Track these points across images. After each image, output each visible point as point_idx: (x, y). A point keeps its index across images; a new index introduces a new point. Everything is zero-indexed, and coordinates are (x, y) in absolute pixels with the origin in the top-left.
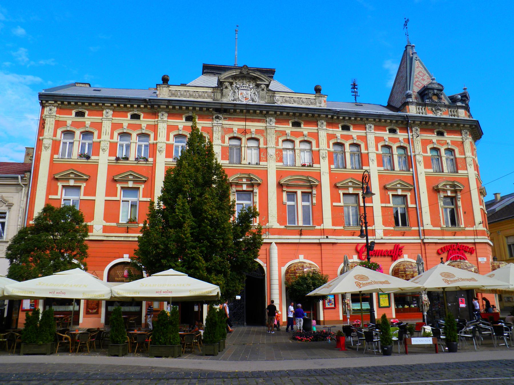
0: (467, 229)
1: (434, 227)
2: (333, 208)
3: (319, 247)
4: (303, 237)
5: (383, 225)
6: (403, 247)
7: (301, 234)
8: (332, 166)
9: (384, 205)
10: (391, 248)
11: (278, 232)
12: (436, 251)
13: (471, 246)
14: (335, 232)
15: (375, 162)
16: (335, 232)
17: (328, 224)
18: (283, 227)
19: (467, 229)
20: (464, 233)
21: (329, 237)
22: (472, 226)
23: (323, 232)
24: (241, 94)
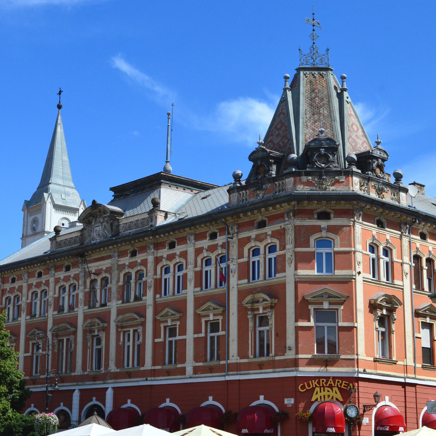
0: (277, 358)
1: (241, 358)
2: (155, 345)
5: (194, 360)
7: (130, 377)
8: (158, 296)
9: (196, 336)
11: (116, 376)
14: (153, 373)
15: (193, 284)
16: (153, 373)
18: (118, 370)
19: (277, 358)
20: (274, 365)
22: (283, 355)
24: (96, 231)
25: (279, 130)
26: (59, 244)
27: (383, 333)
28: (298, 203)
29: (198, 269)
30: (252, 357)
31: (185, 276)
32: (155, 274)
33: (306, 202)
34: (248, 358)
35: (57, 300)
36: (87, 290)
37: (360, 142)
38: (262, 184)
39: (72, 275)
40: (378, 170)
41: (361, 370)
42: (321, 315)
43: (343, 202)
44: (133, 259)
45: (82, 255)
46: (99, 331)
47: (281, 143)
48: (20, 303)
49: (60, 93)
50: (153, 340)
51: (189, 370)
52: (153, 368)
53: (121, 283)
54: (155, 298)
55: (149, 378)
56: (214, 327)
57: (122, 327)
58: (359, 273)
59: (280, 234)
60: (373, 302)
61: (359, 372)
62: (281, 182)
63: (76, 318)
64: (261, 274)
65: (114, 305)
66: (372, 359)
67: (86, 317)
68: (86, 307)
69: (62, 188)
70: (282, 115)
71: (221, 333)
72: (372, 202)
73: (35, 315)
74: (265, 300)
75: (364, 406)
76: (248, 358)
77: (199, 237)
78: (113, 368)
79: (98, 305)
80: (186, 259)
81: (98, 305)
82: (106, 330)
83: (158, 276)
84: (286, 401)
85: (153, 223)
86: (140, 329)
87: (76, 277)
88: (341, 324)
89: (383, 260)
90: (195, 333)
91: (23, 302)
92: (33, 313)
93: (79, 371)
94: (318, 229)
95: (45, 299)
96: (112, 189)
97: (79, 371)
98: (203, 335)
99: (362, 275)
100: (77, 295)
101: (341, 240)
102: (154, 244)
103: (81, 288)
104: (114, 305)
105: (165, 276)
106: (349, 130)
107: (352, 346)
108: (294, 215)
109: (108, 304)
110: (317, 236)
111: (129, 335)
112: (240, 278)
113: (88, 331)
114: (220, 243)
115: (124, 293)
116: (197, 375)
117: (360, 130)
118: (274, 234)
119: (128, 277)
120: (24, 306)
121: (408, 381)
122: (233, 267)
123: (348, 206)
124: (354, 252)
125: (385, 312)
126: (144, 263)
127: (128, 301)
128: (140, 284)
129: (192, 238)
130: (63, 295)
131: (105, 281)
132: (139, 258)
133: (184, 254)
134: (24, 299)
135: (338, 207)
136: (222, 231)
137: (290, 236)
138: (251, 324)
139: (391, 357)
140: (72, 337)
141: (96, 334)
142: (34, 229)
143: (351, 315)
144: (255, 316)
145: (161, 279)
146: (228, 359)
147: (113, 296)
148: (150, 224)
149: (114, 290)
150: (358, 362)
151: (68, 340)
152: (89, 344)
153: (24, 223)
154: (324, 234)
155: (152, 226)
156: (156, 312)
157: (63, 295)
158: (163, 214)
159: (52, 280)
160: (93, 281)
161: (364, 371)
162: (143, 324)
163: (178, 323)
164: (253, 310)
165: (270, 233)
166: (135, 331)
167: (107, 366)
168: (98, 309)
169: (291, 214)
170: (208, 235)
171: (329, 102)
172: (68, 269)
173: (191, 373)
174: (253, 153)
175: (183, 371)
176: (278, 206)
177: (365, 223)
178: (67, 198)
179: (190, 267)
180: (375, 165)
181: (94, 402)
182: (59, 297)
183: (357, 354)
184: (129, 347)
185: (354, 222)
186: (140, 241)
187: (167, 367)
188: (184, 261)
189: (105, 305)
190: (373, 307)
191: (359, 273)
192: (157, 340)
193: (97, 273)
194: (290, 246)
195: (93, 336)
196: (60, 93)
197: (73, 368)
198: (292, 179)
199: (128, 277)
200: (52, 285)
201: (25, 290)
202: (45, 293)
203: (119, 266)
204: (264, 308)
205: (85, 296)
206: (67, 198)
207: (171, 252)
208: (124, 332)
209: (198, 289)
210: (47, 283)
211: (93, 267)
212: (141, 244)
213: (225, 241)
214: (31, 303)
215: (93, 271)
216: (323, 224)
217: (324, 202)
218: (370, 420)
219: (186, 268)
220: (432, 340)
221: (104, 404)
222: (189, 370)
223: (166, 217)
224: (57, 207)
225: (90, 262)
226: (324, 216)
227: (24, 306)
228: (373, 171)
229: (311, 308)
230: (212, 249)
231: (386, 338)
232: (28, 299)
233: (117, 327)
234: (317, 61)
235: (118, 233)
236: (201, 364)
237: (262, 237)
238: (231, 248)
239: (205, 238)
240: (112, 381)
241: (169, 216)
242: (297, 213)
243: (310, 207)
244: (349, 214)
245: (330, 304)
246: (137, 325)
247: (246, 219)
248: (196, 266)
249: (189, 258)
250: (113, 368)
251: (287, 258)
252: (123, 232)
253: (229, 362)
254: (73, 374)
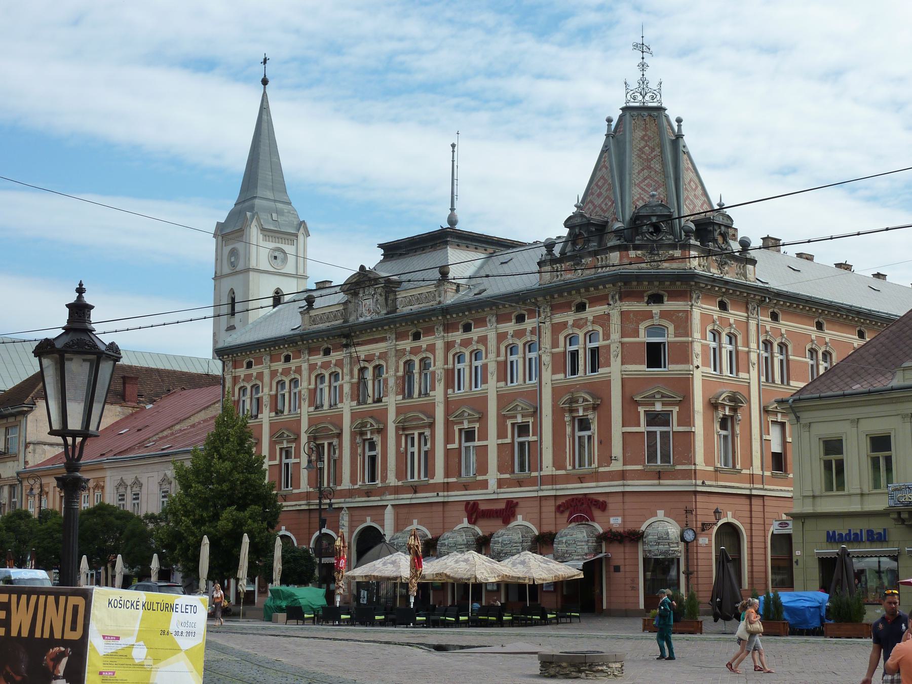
0: (601, 469)
1: (557, 469)
2: (447, 452)
3: (441, 508)
4: (418, 495)
5: (498, 471)
6: (517, 503)
7: (415, 492)
8: (450, 391)
9: (500, 441)
10: (502, 506)
11: (396, 490)
12: (553, 509)
13: (601, 499)
14: (447, 487)
15: (495, 377)
16: (447, 487)
17: (439, 477)
18: (400, 483)
19: (601, 469)
20: (596, 476)
21: (440, 494)
22: (608, 466)
23: (434, 488)
25: (600, 188)
26: (314, 321)
27: (725, 437)
28: (625, 284)
29: (502, 358)
30: (571, 468)
31: (485, 367)
32: (446, 362)
33: (635, 283)
34: (566, 469)
35: (313, 393)
36: (355, 380)
37: (699, 203)
38: (581, 258)
39: (334, 362)
40: (720, 240)
41: (699, 482)
42: (654, 419)
43: (678, 283)
44: (416, 344)
45: (347, 336)
46: (372, 433)
47: (603, 206)
48: (260, 395)
49: (265, 61)
50: (445, 446)
51: (492, 484)
52: (446, 480)
53: (401, 373)
54: (446, 393)
55: (440, 494)
56: (523, 429)
57: (404, 429)
58: (698, 367)
59: (603, 320)
60: (713, 402)
61: (696, 485)
62: (603, 256)
63: (341, 417)
64: (581, 368)
65: (392, 401)
66: (711, 469)
67: (354, 416)
68: (355, 403)
69: (272, 204)
70: (604, 169)
71: (531, 438)
72: (714, 280)
73: (282, 412)
74: (585, 400)
75: (703, 524)
76: (566, 469)
77: (501, 319)
78: (392, 480)
79: (370, 400)
80: (486, 346)
81: (370, 400)
82: (382, 431)
83: (450, 366)
84: (612, 520)
85: (442, 299)
86: (427, 432)
87: (339, 364)
88: (676, 428)
89: (727, 347)
90: (499, 437)
91: (265, 393)
92: (280, 407)
93: (346, 484)
95: (296, 390)
96: (380, 246)
97: (346, 484)
98: (509, 440)
99: (701, 369)
100: (341, 386)
101: (676, 328)
102: (444, 325)
103: (347, 378)
104: (392, 401)
105: (458, 366)
106: (686, 189)
107: (687, 453)
108: (621, 299)
109: (384, 399)
110: (648, 323)
111: (413, 439)
112: (554, 373)
113: (359, 432)
114: (529, 328)
115: (406, 385)
116: (502, 490)
117: (700, 187)
118: (597, 320)
119: (409, 364)
120: (266, 400)
121: (754, 492)
122: (546, 359)
124: (692, 342)
125: (728, 411)
126: (431, 348)
127: (410, 395)
128: (426, 374)
129: (494, 319)
130: (321, 386)
131: (378, 368)
132: (424, 342)
133: (483, 340)
134: (266, 390)
135: (672, 288)
136: (532, 314)
137: (615, 320)
138: (569, 430)
139: (734, 466)
140: (335, 442)
141: (369, 437)
142: (233, 265)
143: (687, 418)
144: (574, 418)
145: (454, 369)
146: (541, 469)
147: (389, 389)
148: (438, 299)
149: (391, 382)
150: (695, 473)
151: (330, 444)
152: (360, 450)
153: (217, 255)
154: (656, 321)
155: (440, 302)
156: (447, 413)
157: (321, 386)
158: (454, 287)
159: (305, 366)
160: (362, 370)
161: (703, 483)
162: (432, 425)
163: (477, 425)
164: (571, 411)
165: (591, 318)
166: (420, 434)
167: (384, 478)
168: (370, 406)
169: (617, 297)
170: (513, 317)
171: (662, 152)
172: (327, 352)
173: (496, 486)
174: (570, 218)
175: (484, 485)
176: (601, 287)
177: (704, 306)
178: (281, 220)
179: (492, 356)
180: (716, 233)
181: (369, 522)
182: (315, 389)
183: (695, 464)
184: (413, 453)
185: (692, 305)
186: (425, 321)
187: (464, 478)
188: (483, 348)
189: (379, 400)
190: (713, 405)
191: (698, 367)
192: (449, 446)
193: (368, 360)
194: (615, 336)
195: (364, 440)
196: (265, 61)
197: (337, 480)
198: (617, 254)
199: (409, 364)
200: (305, 373)
201: (266, 379)
202: (295, 382)
203: (397, 351)
204: (585, 410)
205: (352, 388)
206: (281, 220)
207: (467, 336)
208: (407, 436)
209: (502, 384)
210: (298, 370)
211: (363, 351)
212: (426, 325)
213: (535, 325)
214: (276, 395)
215: (363, 357)
216: (655, 309)
217: (656, 283)
218: (710, 540)
219: (486, 358)
220: (784, 443)
221: (383, 526)
222: (492, 484)
223: (457, 291)
225: (358, 344)
226: (657, 299)
227: (266, 400)
228: (715, 241)
229: (641, 410)
230: (519, 334)
231: (728, 442)
232: (271, 390)
233: (397, 429)
234: (647, 98)
235: (395, 310)
236: (507, 476)
237: (582, 322)
238: (543, 335)
239: (510, 321)
240: (392, 497)
241: (461, 288)
242: (624, 296)
243: (640, 289)
245: (663, 404)
246: (424, 427)
247: (562, 300)
248: (498, 355)
249: (489, 344)
250: (392, 480)
251: (612, 350)
252: (404, 310)
253: (542, 473)
254: (339, 488)
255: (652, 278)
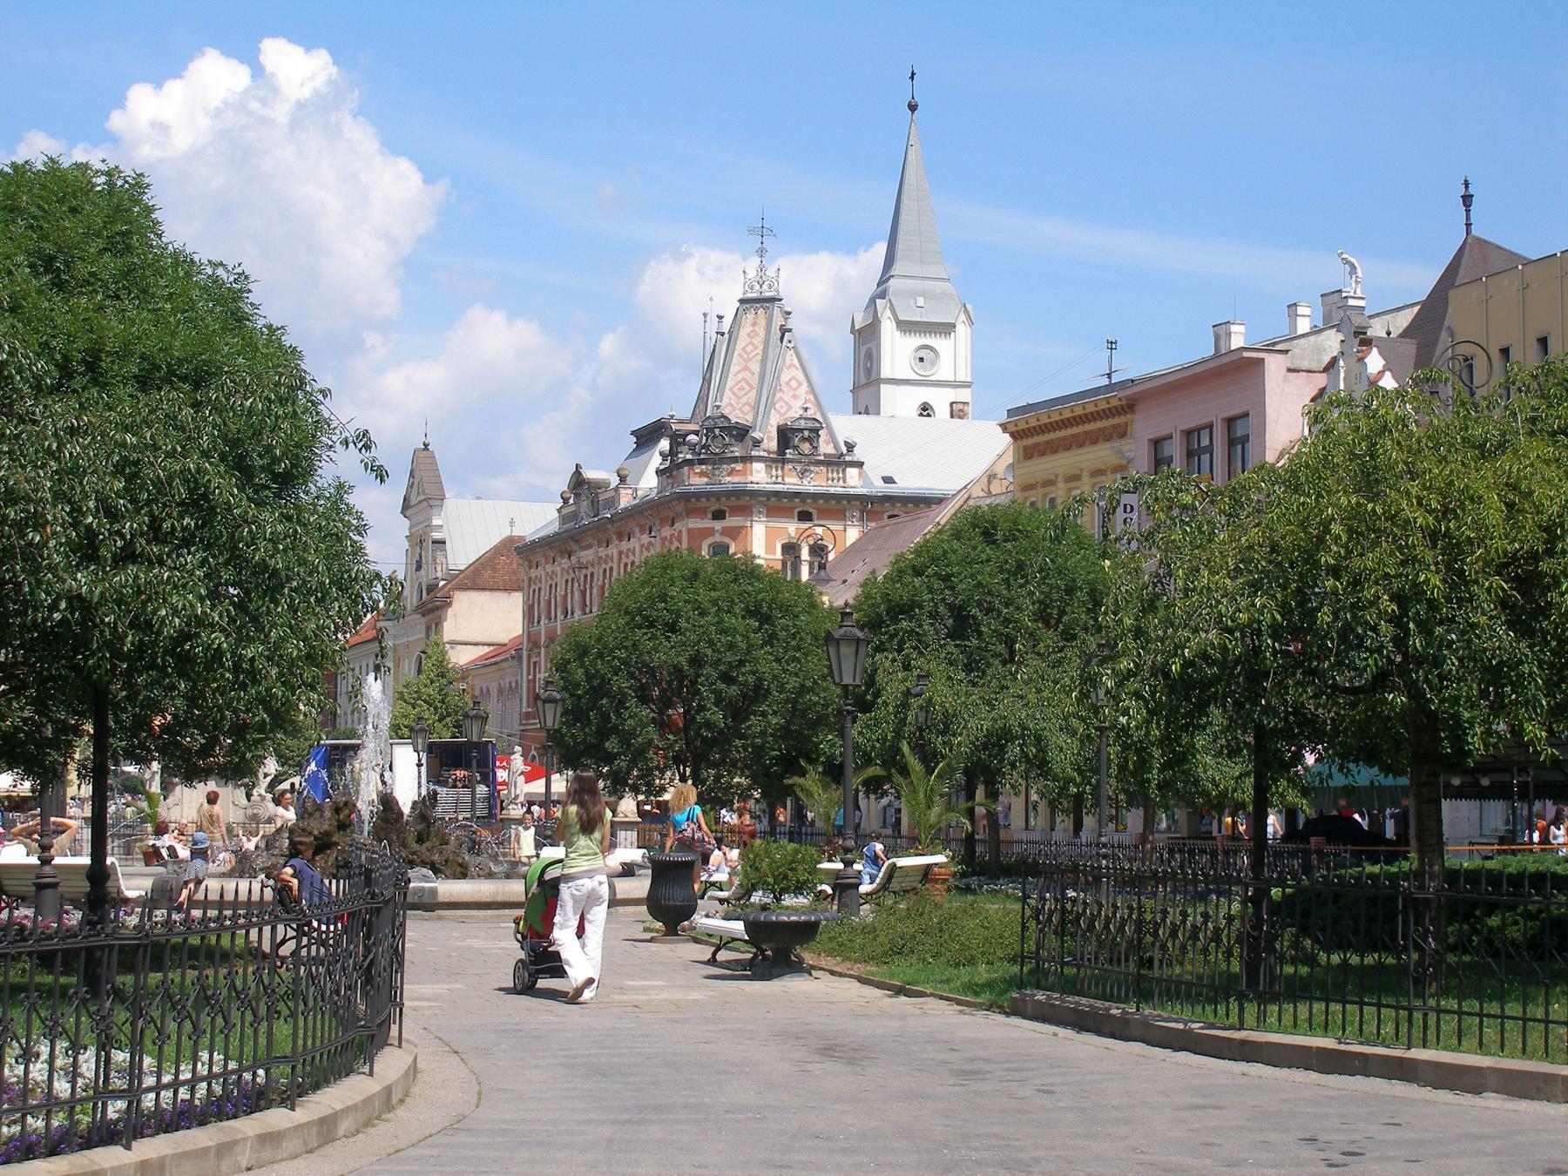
94: (711, 532)
110: (710, 540)
123: (741, 503)
154: (718, 538)
216: (718, 525)
224: (906, 327)
226: (719, 515)
242: (691, 513)
244: (746, 511)
255: (709, 495)
